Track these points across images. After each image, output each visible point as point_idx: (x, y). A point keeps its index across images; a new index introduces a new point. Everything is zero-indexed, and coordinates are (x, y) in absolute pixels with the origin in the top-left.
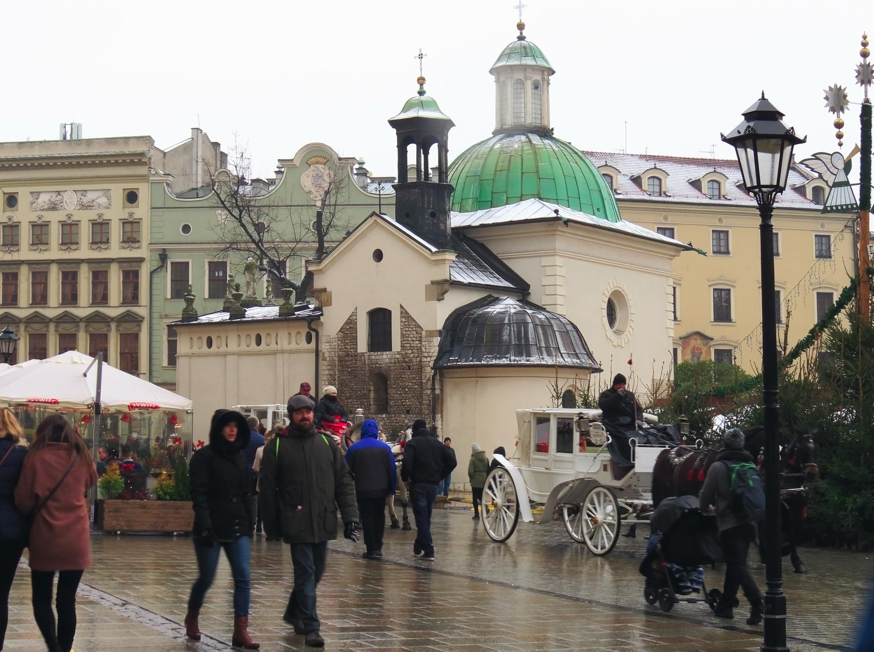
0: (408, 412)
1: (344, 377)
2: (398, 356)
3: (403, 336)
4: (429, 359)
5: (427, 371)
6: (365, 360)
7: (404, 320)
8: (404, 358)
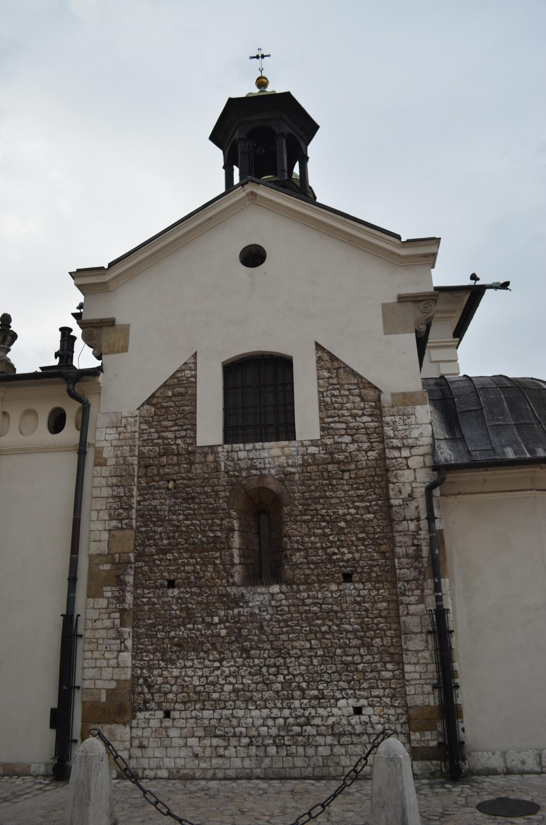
0: (348, 578)
1: (154, 503)
2: (313, 450)
3: (324, 406)
4: (405, 453)
5: (402, 479)
6: (216, 462)
7: (326, 374)
8: (331, 454)
